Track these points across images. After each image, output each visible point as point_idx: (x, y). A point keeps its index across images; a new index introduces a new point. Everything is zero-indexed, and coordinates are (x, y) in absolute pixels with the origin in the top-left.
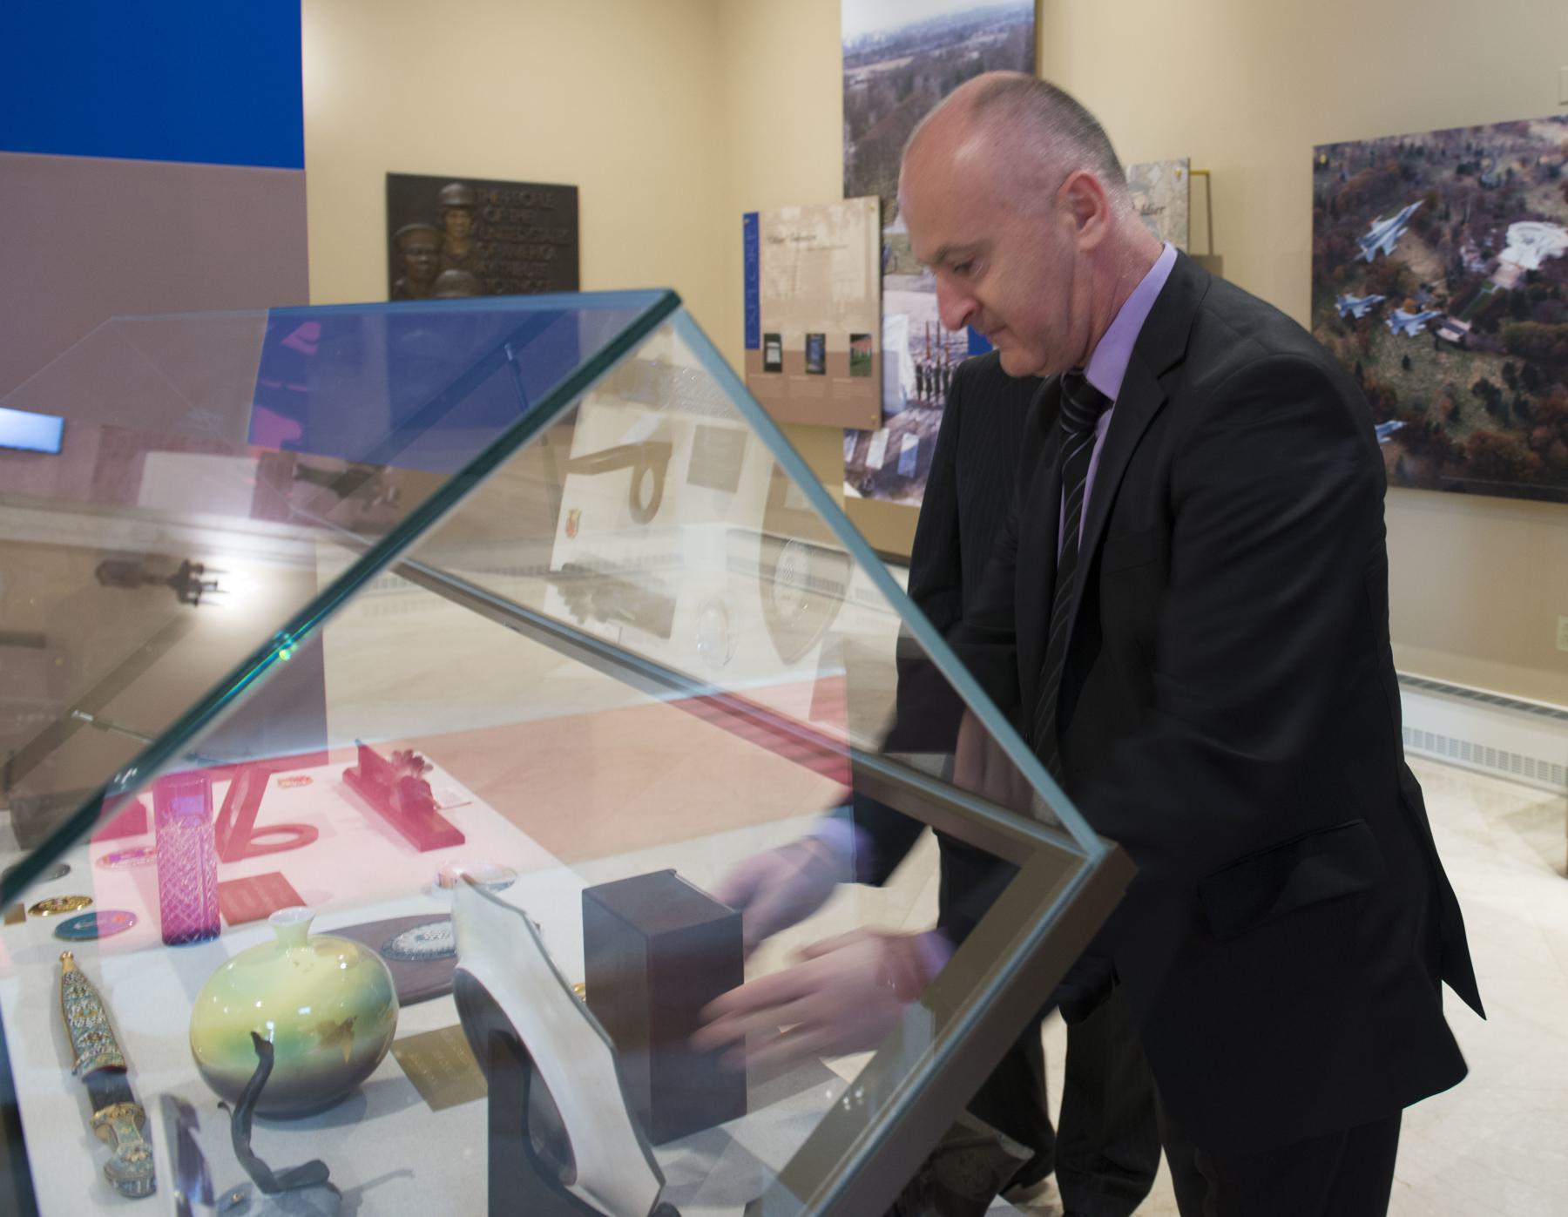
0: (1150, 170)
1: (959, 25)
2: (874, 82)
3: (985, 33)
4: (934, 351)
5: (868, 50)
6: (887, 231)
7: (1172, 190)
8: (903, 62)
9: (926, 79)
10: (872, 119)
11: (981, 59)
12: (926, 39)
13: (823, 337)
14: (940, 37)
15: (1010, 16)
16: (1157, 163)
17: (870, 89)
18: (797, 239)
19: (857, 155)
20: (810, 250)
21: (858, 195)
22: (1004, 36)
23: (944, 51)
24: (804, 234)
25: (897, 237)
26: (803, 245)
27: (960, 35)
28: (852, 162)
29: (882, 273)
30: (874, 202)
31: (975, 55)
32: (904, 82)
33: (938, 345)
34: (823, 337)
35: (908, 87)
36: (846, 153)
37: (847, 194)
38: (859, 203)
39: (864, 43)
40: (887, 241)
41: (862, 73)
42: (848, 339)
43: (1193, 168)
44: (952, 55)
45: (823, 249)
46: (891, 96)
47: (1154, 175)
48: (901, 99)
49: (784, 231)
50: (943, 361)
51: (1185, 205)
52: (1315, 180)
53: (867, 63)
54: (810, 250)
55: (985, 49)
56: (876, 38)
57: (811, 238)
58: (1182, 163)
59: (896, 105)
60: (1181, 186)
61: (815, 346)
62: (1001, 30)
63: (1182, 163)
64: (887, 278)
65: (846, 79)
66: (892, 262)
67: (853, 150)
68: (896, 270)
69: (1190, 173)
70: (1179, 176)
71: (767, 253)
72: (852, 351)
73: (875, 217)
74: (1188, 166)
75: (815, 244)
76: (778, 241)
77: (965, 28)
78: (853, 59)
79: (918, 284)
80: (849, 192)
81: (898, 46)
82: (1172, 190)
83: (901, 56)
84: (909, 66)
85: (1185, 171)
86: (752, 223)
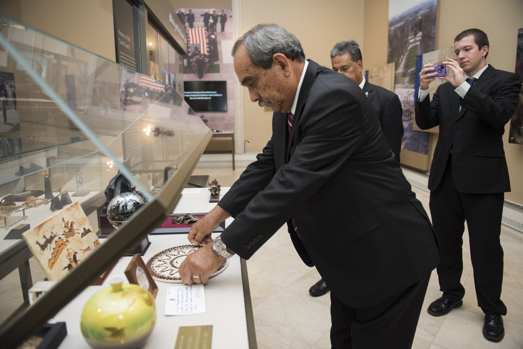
1: (416, 10)
2: (395, 30)
3: (423, 10)
4: (406, 105)
5: (394, 21)
6: (397, 72)
8: (402, 23)
9: (408, 27)
10: (395, 41)
11: (421, 19)
12: (408, 15)
14: (411, 14)
15: (430, 3)
17: (394, 32)
18: (376, 76)
22: (428, 10)
23: (412, 18)
24: (378, 75)
25: (399, 73)
26: (377, 78)
27: (416, 12)
30: (393, 64)
31: (420, 17)
32: (402, 28)
33: (407, 103)
35: (403, 30)
36: (388, 52)
38: (390, 65)
39: (393, 20)
41: (393, 28)
44: (414, 18)
45: (382, 79)
46: (399, 33)
48: (401, 34)
49: (373, 75)
50: (408, 107)
53: (394, 25)
54: (379, 79)
55: (423, 15)
56: (397, 17)
59: (400, 36)
62: (427, 9)
65: (389, 30)
67: (390, 50)
68: (399, 83)
73: (394, 68)
75: (380, 77)
76: (372, 77)
77: (418, 10)
78: (391, 24)
79: (403, 86)
80: (389, 62)
81: (401, 19)
83: (402, 22)
84: (404, 24)
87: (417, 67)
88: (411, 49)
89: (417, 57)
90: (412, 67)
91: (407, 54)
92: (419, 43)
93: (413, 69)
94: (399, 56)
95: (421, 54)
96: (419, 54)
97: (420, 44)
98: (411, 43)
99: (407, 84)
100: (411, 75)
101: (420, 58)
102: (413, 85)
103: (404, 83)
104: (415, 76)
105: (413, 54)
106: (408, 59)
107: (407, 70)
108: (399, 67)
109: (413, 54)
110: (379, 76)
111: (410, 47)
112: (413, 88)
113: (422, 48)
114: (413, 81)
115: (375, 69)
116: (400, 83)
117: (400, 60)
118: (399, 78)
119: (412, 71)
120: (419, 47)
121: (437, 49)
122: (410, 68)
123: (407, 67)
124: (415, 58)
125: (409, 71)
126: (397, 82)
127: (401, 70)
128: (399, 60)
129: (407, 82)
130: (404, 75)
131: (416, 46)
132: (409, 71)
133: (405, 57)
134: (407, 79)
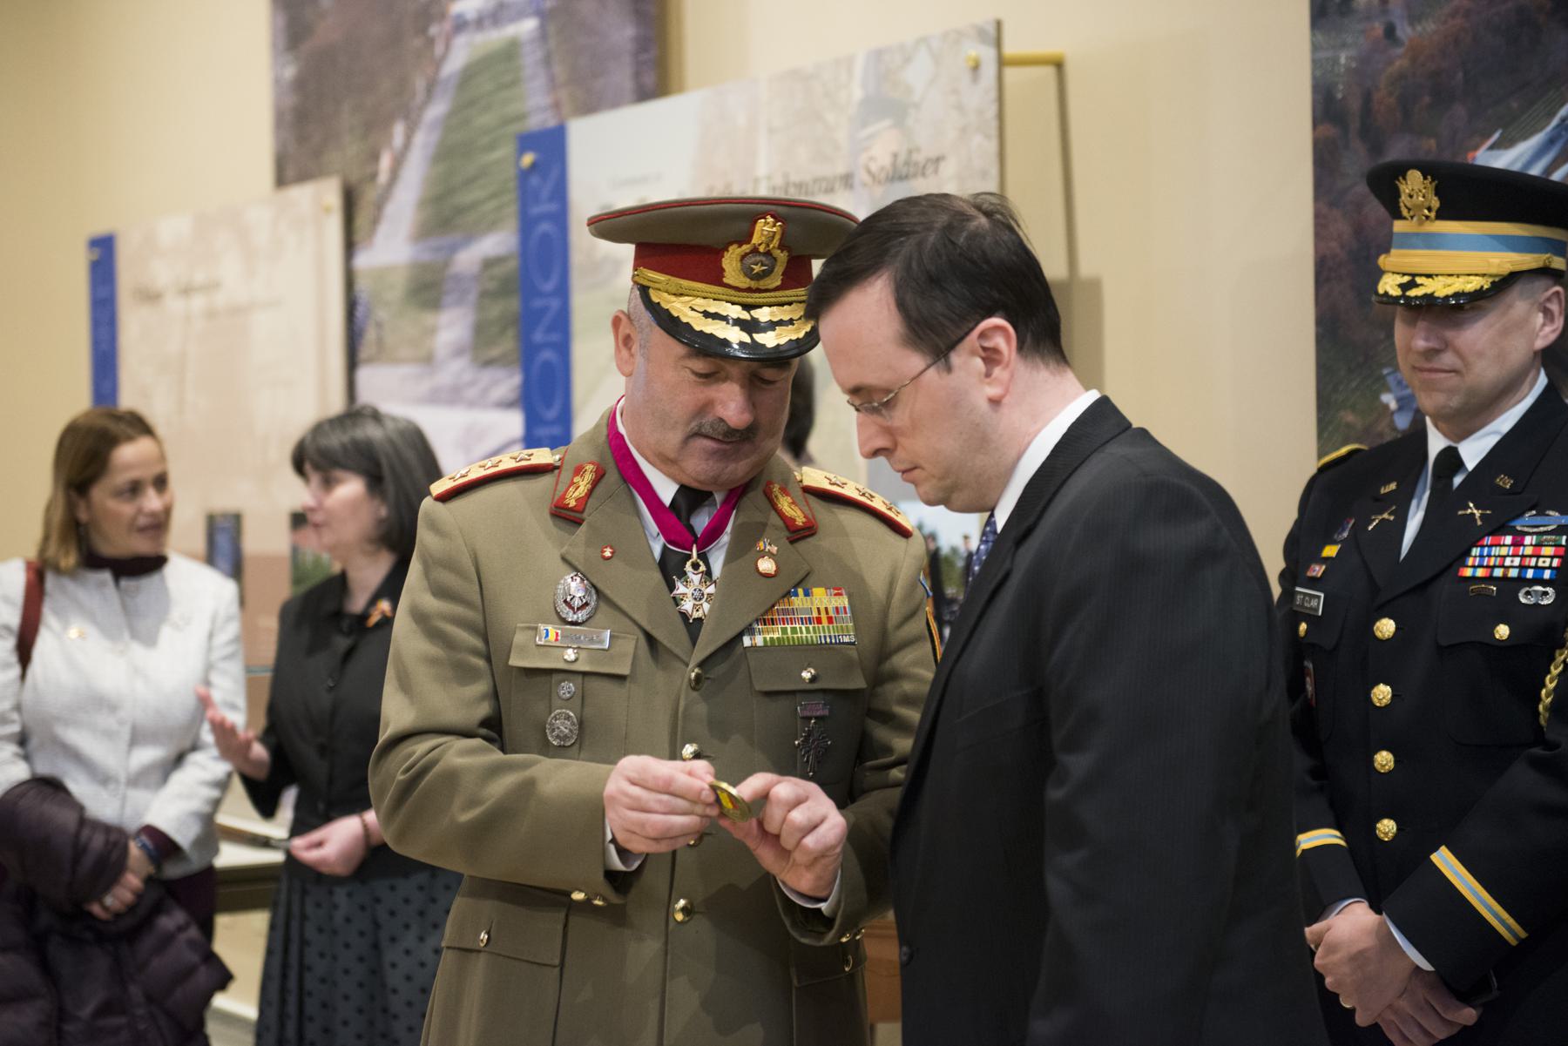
0: (908, 60)
6: (362, 261)
7: (960, 108)
13: (236, 519)
16: (924, 40)
18: (187, 291)
19: (300, 84)
20: (211, 314)
21: (304, 177)
24: (199, 278)
25: (381, 274)
26: (198, 302)
28: (290, 100)
29: (352, 362)
30: (328, 193)
34: (236, 519)
36: (277, 81)
37: (281, 181)
40: (363, 286)
42: (284, 523)
43: (1010, 50)
45: (237, 311)
47: (917, 75)
49: (162, 274)
51: (992, 146)
52: (1315, 48)
54: (211, 314)
57: (212, 286)
58: (981, 34)
60: (980, 96)
61: (223, 541)
63: (981, 34)
64: (364, 375)
66: (370, 335)
67: (290, 72)
68: (383, 355)
69: (1002, 62)
70: (976, 67)
71: (132, 324)
72: (295, 551)
74: (998, 43)
75: (220, 299)
76: (151, 297)
79: (425, 387)
80: (287, 173)
82: (960, 108)
85: (988, 55)
86: (104, 253)
87: (527, 226)
88: (468, 75)
89: (527, 142)
90: (492, 226)
91: (436, 110)
92: (529, 25)
93: (498, 242)
94: (375, 126)
95: (552, 123)
96: (538, 121)
97: (543, 35)
98: (461, 25)
99: (455, 370)
100: (484, 295)
101: (550, 148)
102: (508, 382)
103: (428, 360)
104: (514, 304)
105: (485, 120)
106: (447, 154)
107: (454, 249)
108: (375, 221)
109: (485, 120)
110: (212, 286)
111: (460, 54)
112: (507, 405)
113: (559, 70)
114: (508, 344)
115: (173, 229)
116: (396, 361)
117: (385, 162)
118: (382, 314)
119: (489, 264)
120: (530, 59)
121: (681, 89)
122: (470, 238)
123: (444, 218)
124: (506, 151)
125: (469, 258)
126: (365, 352)
127: (392, 248)
128: (375, 157)
129: (458, 352)
130: (428, 289)
131: (510, 52)
132: (469, 258)
133: (424, 141)
134: (452, 327)
